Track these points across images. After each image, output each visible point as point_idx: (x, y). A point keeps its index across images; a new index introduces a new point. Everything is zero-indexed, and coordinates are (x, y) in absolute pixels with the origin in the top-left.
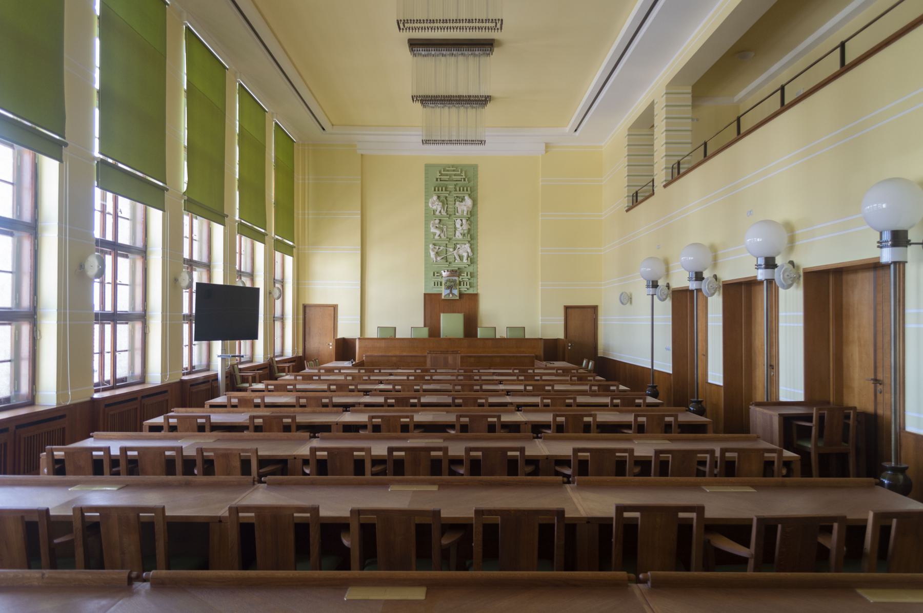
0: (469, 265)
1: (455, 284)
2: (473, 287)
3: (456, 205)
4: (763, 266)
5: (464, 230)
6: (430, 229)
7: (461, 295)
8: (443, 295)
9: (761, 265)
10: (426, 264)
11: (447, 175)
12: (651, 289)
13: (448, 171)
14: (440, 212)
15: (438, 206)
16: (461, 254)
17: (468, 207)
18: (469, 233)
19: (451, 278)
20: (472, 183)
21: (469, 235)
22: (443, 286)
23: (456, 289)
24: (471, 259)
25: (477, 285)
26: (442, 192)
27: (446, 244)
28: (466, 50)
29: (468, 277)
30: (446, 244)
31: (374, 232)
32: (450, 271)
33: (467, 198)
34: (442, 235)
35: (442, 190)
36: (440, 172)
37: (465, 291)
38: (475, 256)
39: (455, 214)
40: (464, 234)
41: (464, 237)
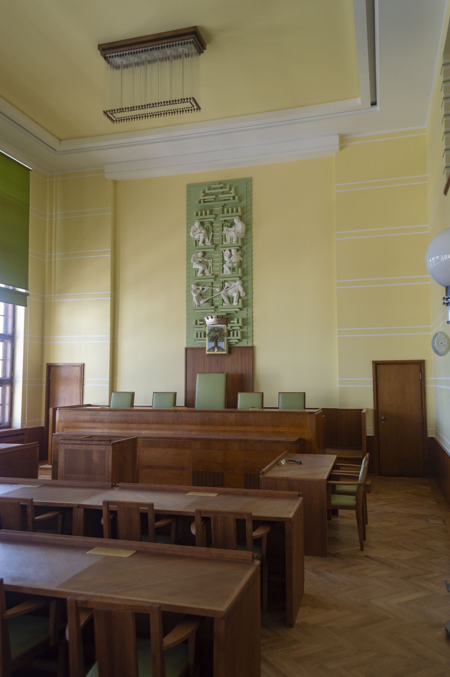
1: (220, 335)
2: (247, 338)
5: (233, 263)
7: (230, 349)
10: (188, 310)
11: (212, 194)
13: (214, 189)
14: (204, 242)
16: (230, 294)
20: (244, 203)
21: (240, 269)
23: (223, 341)
25: (253, 336)
27: (212, 283)
30: (212, 283)
33: (236, 221)
34: (207, 271)
35: (206, 214)
36: (204, 192)
37: (236, 343)
38: (249, 297)
39: (222, 243)
41: (234, 273)
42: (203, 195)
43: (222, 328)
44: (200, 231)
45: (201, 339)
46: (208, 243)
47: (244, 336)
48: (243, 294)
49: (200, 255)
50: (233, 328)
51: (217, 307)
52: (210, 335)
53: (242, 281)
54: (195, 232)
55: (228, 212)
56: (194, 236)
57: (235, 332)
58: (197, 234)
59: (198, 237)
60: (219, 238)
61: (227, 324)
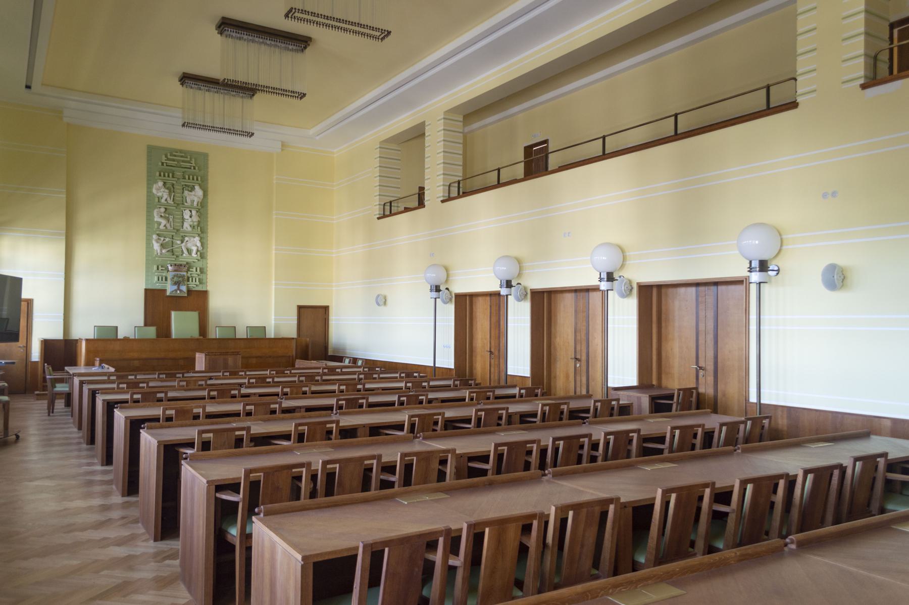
0: (198, 260)
4: (606, 279)
6: (154, 217)
7: (189, 291)
9: (603, 279)
10: (147, 256)
11: (174, 160)
12: (434, 293)
13: (175, 156)
14: (166, 200)
15: (164, 193)
17: (199, 198)
18: (198, 226)
21: (199, 228)
24: (201, 253)
27: (173, 236)
28: (257, 37)
29: (196, 273)
30: (173, 236)
31: (83, 217)
33: (197, 187)
34: (168, 225)
35: (169, 176)
36: (166, 156)
37: (194, 287)
38: (205, 250)
39: (183, 204)
40: (194, 226)
41: (194, 230)
47: (201, 281)
48: (200, 248)
51: (177, 257)
54: (158, 190)
56: (158, 193)
57: (194, 279)
58: (161, 192)
61: (187, 272)
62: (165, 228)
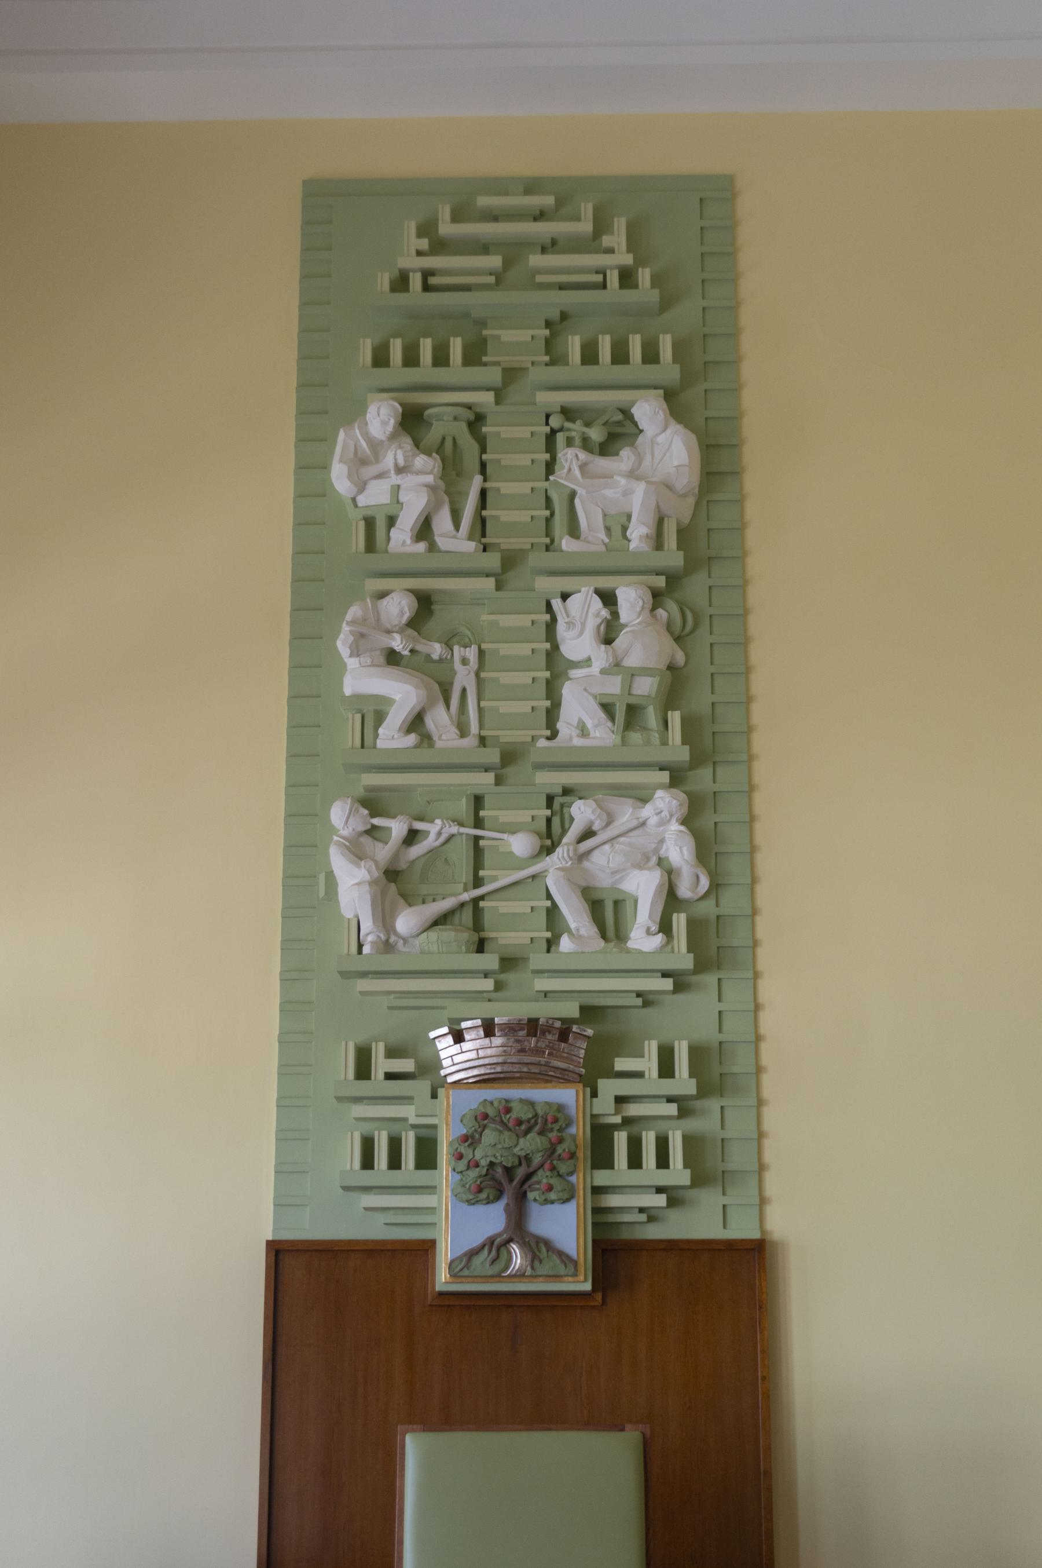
1: (551, 1151)
3: (560, 476)
5: (633, 674)
8: (445, 1255)
11: (484, 248)
13: (493, 216)
14: (424, 530)
15: (408, 481)
16: (603, 881)
19: (514, 1093)
21: (675, 718)
22: (445, 1174)
24: (693, 925)
25: (762, 1168)
26: (441, 375)
27: (478, 801)
29: (669, 1087)
30: (478, 801)
32: (510, 1029)
34: (439, 720)
35: (441, 359)
36: (426, 229)
37: (651, 1215)
38: (731, 902)
41: (635, 737)
42: (424, 244)
43: (561, 1108)
44: (406, 458)
45: (396, 1178)
46: (454, 537)
49: (402, 613)
50: (633, 1110)
51: (509, 963)
52: (479, 1154)
53: (685, 792)
54: (364, 462)
55: (590, 356)
56: (362, 487)
59: (385, 499)
60: (523, 516)
62: (412, 739)
